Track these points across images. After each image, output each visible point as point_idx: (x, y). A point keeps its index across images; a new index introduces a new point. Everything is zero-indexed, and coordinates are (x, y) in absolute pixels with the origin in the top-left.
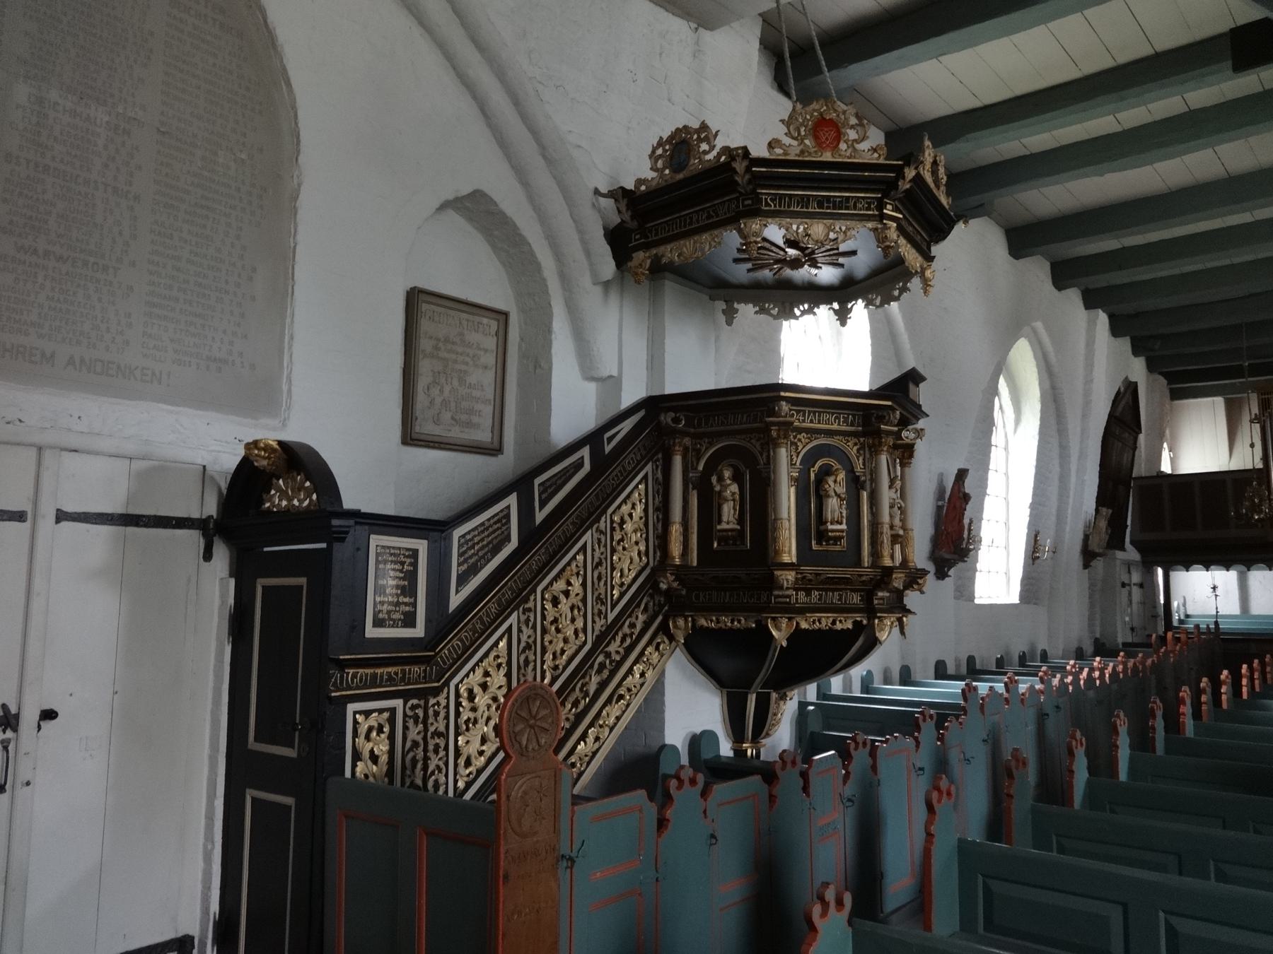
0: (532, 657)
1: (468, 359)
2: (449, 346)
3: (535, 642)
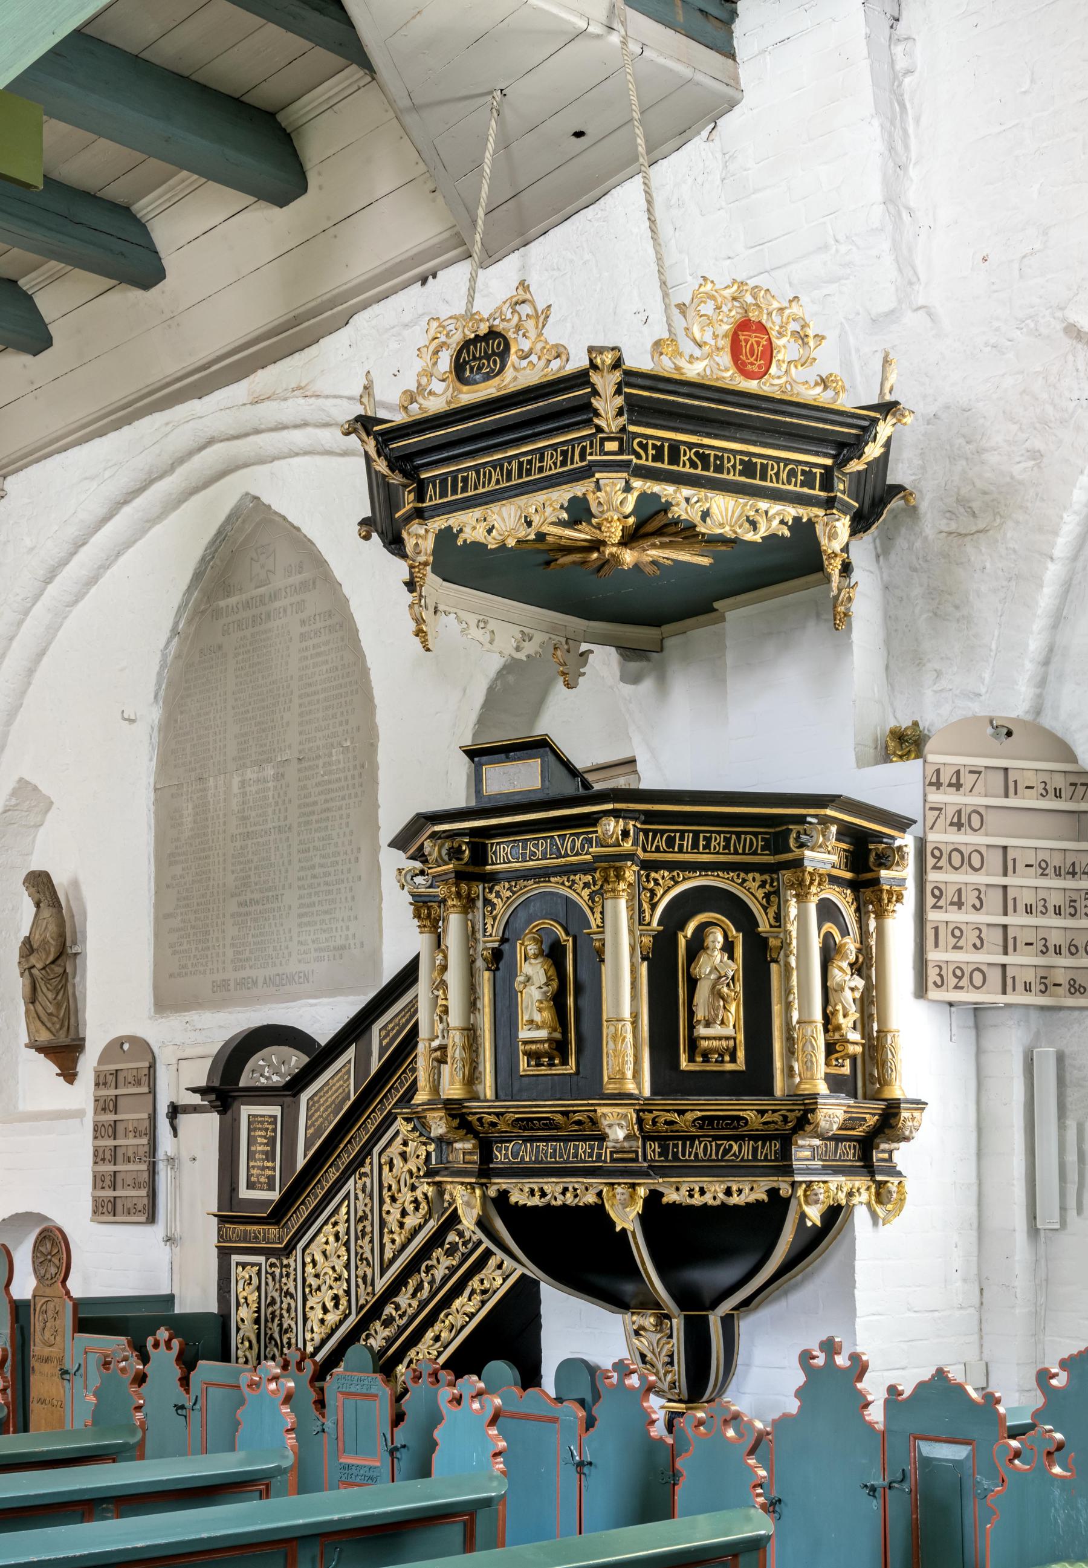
0: (368, 1229)
3: (372, 1210)
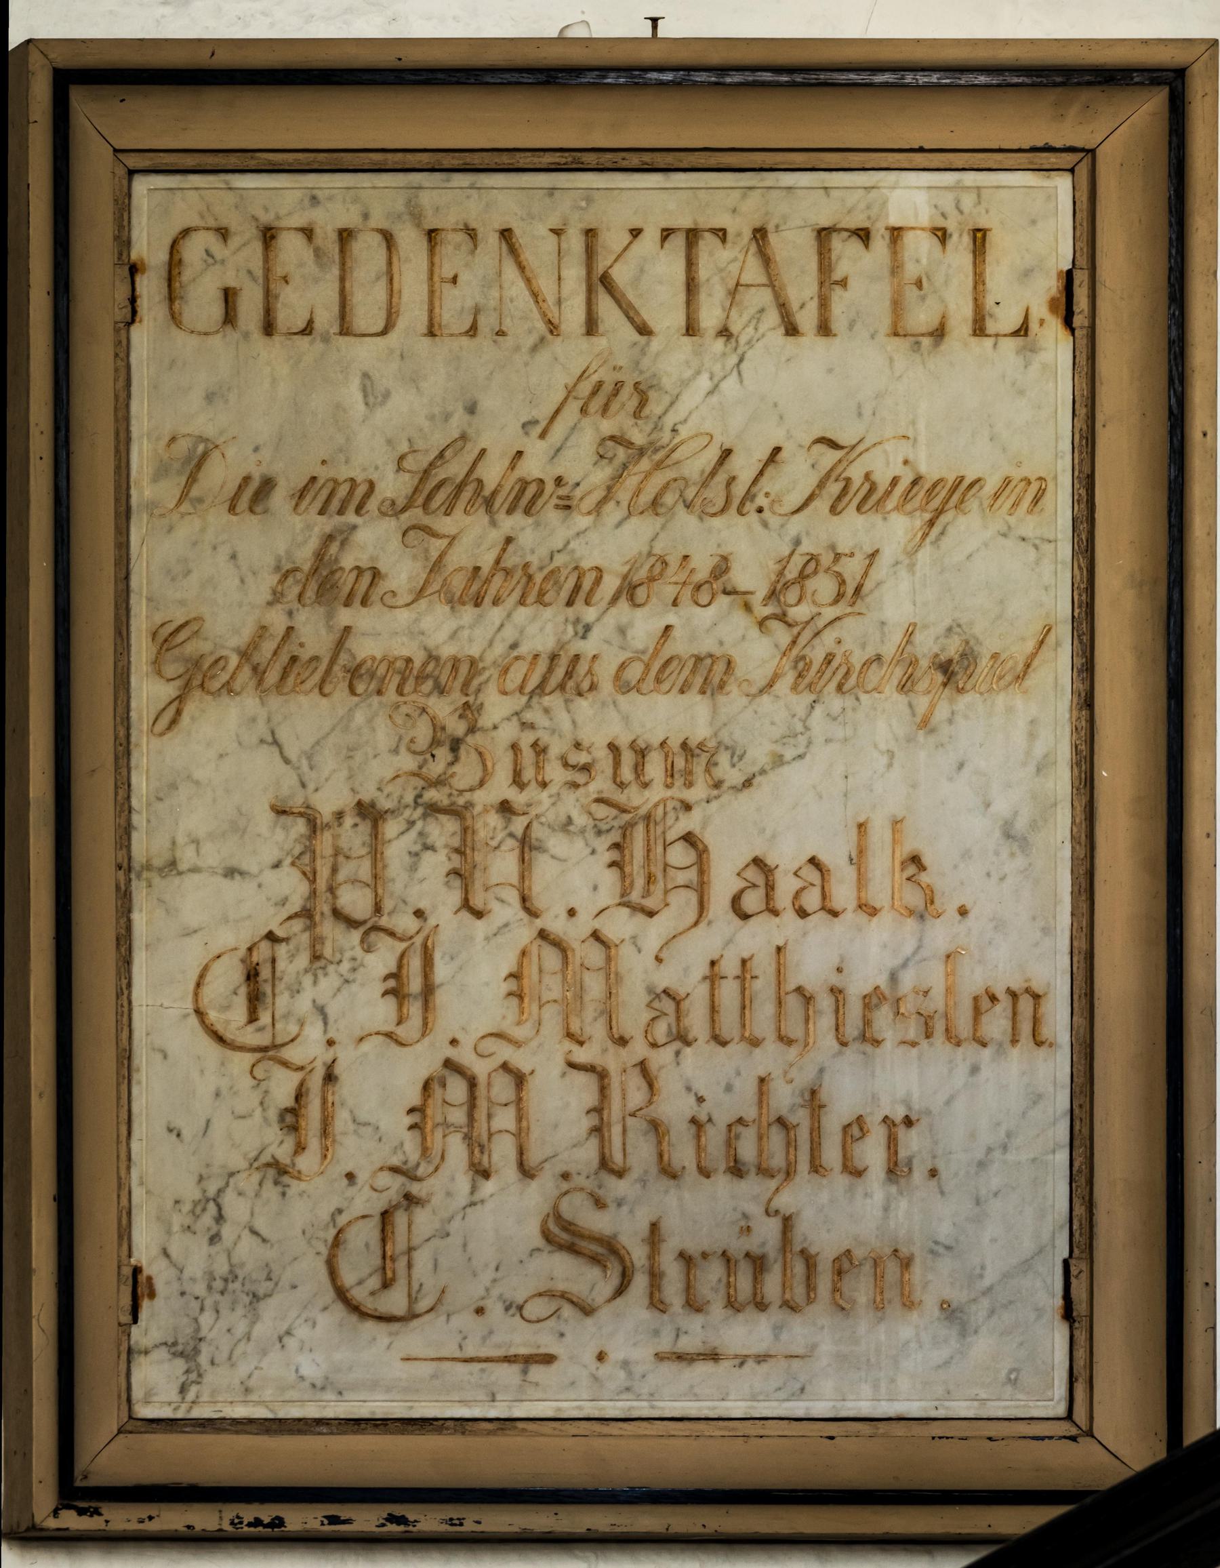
1: (709, 626)
2: (473, 538)
